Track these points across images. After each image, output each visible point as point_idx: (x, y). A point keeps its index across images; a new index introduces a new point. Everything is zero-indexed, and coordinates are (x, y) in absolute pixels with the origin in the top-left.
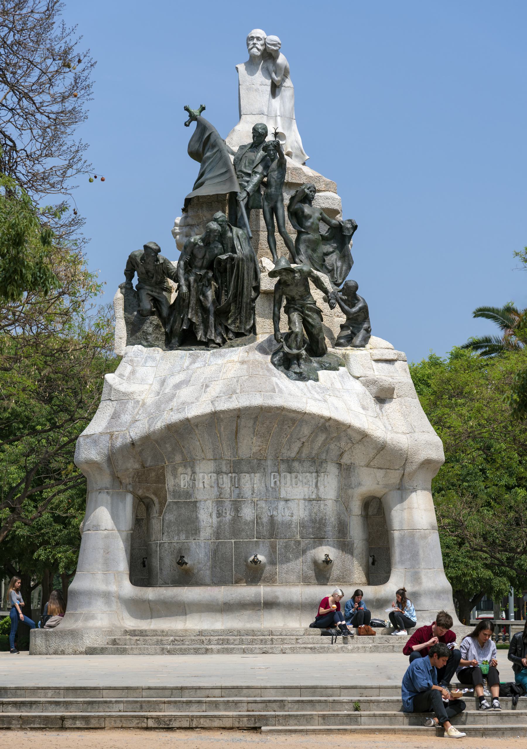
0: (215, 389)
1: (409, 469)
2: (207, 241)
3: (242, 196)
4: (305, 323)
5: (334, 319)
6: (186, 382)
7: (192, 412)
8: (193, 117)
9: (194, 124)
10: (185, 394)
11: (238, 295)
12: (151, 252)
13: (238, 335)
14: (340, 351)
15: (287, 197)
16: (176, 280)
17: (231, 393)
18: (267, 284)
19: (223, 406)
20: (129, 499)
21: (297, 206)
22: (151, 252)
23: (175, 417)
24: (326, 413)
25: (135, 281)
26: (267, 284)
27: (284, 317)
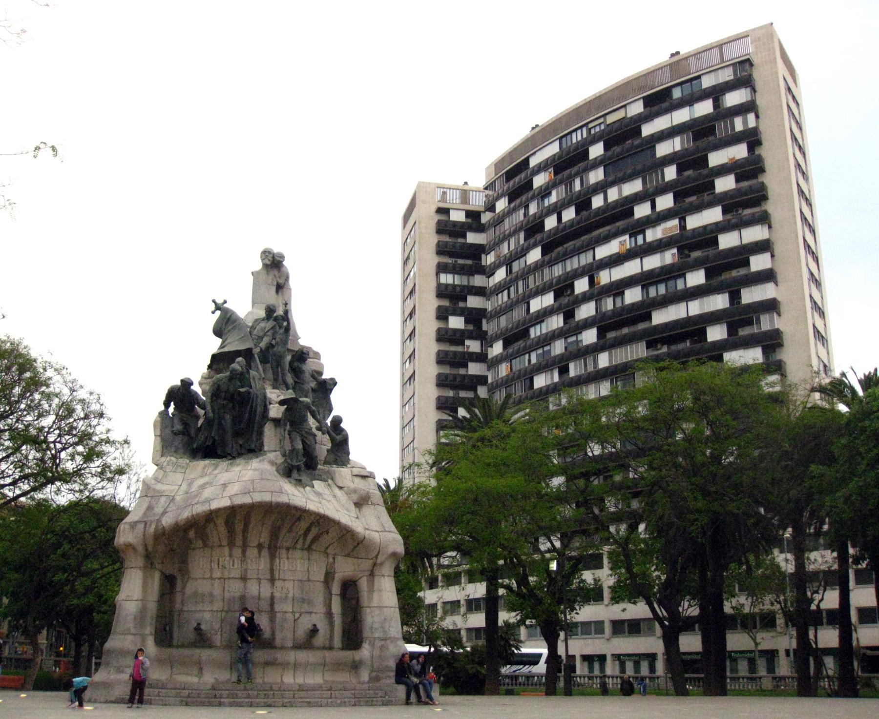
0: (234, 489)
2: (231, 379)
3: (256, 351)
4: (303, 442)
5: (323, 444)
7: (214, 505)
9: (218, 313)
10: (207, 493)
11: (251, 421)
12: (186, 384)
14: (326, 468)
16: (203, 407)
18: (276, 411)
19: (239, 501)
20: (157, 575)
21: (296, 364)
22: (186, 384)
23: (200, 509)
24: (322, 511)
25: (171, 409)
26: (276, 411)
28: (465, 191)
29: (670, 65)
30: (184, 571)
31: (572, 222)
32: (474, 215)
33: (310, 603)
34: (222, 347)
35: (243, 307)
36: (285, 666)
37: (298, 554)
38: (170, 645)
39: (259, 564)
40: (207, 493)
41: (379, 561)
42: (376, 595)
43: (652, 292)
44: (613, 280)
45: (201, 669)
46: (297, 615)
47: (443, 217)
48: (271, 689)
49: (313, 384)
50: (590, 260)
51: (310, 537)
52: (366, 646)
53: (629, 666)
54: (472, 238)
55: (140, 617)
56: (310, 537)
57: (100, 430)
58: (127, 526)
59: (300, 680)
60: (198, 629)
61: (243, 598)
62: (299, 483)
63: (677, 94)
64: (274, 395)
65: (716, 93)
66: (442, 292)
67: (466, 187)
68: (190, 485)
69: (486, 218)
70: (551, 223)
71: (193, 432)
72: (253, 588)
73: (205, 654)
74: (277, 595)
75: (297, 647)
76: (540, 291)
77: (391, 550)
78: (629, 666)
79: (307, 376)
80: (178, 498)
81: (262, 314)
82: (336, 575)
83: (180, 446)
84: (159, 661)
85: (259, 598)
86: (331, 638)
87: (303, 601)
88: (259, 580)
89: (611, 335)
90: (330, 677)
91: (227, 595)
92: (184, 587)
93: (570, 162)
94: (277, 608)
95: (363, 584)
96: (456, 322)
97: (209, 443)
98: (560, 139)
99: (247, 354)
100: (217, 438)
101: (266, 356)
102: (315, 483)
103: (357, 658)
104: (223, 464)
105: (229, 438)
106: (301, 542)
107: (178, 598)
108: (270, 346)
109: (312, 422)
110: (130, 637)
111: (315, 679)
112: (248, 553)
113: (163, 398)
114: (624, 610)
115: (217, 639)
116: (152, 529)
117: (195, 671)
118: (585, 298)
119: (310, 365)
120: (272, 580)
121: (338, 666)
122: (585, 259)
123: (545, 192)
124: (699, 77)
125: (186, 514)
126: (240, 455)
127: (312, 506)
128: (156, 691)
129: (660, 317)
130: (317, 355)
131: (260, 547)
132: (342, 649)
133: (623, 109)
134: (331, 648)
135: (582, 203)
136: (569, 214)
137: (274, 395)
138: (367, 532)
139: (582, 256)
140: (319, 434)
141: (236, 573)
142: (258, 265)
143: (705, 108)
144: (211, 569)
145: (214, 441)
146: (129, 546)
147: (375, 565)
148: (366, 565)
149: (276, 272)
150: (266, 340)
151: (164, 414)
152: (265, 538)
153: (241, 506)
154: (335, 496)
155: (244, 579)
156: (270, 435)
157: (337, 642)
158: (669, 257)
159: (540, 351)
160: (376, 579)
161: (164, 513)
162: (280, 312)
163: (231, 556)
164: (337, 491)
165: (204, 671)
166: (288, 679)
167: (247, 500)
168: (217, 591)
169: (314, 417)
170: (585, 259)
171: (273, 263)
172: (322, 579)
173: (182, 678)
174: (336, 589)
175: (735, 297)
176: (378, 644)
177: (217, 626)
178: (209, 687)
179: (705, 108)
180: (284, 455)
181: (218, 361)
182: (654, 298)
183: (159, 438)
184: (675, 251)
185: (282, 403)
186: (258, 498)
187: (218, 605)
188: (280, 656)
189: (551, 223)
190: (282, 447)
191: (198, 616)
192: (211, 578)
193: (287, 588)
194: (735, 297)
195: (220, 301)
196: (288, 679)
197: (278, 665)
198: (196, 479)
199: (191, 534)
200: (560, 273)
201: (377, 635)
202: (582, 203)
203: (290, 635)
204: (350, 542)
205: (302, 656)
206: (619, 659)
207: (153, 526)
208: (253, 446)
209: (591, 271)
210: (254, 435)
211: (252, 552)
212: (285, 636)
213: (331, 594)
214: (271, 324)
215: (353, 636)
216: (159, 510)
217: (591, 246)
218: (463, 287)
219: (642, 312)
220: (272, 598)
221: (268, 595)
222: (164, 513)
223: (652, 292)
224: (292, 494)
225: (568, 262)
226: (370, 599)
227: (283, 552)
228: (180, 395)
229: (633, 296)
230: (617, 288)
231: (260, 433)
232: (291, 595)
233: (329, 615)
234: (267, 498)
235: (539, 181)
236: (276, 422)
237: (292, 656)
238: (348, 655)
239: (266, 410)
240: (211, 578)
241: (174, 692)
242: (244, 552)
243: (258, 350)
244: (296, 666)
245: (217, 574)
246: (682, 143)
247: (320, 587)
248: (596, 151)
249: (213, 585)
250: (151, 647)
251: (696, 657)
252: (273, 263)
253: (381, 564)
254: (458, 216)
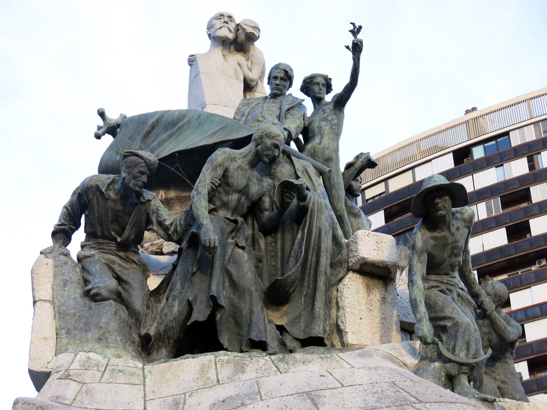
11: (309, 269)
13: (317, 342)
29: (467, 122)
63: (478, 153)
65: (530, 151)
83: (113, 325)
100: (222, 301)
124: (507, 134)
133: (411, 171)
143: (519, 168)
145: (215, 305)
149: (239, 57)
179: (519, 168)
183: (47, 310)
195: (113, 116)
208: (318, 330)
246: (489, 209)
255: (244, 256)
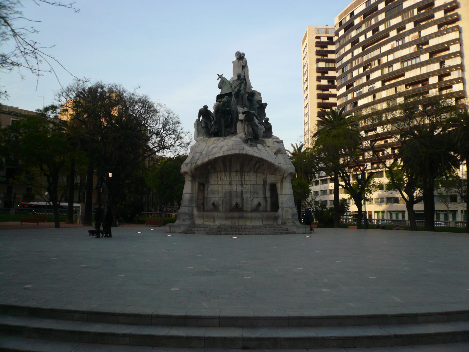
0: (225, 149)
1: (285, 175)
4: (253, 129)
5: (262, 129)
6: (216, 147)
7: (217, 156)
8: (220, 78)
9: (220, 79)
12: (206, 107)
14: (263, 139)
15: (247, 95)
16: (213, 117)
17: (229, 150)
19: (227, 153)
20: (197, 184)
21: (250, 98)
22: (206, 107)
23: (211, 157)
24: (260, 157)
25: (201, 118)
26: (241, 117)
27: (246, 128)
28: (327, 29)
30: (208, 182)
31: (371, 38)
32: (330, 39)
33: (257, 193)
34: (221, 92)
35: (229, 76)
36: (247, 218)
37: (252, 174)
38: (204, 211)
39: (236, 178)
40: (215, 150)
41: (285, 176)
42: (284, 190)
43: (405, 64)
44: (389, 60)
45: (214, 220)
46: (252, 198)
47: (318, 40)
48: (241, 228)
49: (258, 106)
50: (379, 53)
51: (256, 168)
52: (280, 210)
53: (394, 215)
54: (330, 48)
55: (191, 200)
56: (256, 168)
57: (179, 129)
58: (185, 165)
59: (253, 224)
60: (213, 204)
61: (230, 192)
62: (251, 145)
64: (240, 110)
66: (319, 70)
67: (327, 27)
68: (209, 147)
69: (335, 39)
70: (362, 39)
71: (209, 126)
72: (234, 188)
73: (216, 214)
74: (244, 190)
75: (253, 211)
76: (357, 67)
77: (290, 171)
78: (394, 215)
79: (255, 102)
80: (203, 153)
81: (236, 78)
82: (268, 182)
84: (199, 217)
85: (237, 192)
86: (266, 207)
87: (254, 192)
88: (236, 185)
89: (387, 84)
90: (265, 223)
91: (224, 191)
92: (207, 188)
93: (371, 11)
94: (244, 195)
95: (279, 185)
96: (324, 82)
97: (216, 130)
98: (366, 2)
99: (229, 95)
101: (238, 95)
102: (258, 145)
103: (276, 215)
104: (221, 139)
105: (223, 128)
106: (253, 169)
107: (206, 192)
108: (239, 91)
109: (256, 121)
110: (187, 208)
111: (258, 223)
112: (232, 175)
113: (198, 114)
114: (391, 193)
115: (221, 208)
116: (193, 166)
117: (212, 221)
118: (376, 69)
119: (256, 97)
120: (242, 185)
121: (268, 218)
122: (377, 52)
123: (359, 26)
125: (206, 160)
126: (228, 135)
127: (256, 155)
128: (197, 229)
129: (409, 75)
130: (259, 94)
131: (237, 172)
132: (271, 211)
134: (266, 211)
135: (375, 29)
136: (370, 34)
137: (240, 110)
138: (279, 165)
139: (375, 51)
140: (259, 125)
141: (227, 182)
142: (235, 59)
144: (218, 181)
146: (186, 173)
147: (283, 178)
148: (279, 177)
150: (237, 88)
151: (198, 120)
152: (238, 168)
153: (228, 156)
154: (266, 150)
155: (231, 184)
156: (240, 126)
157: (269, 209)
158: (412, 49)
159: (358, 92)
160: (284, 183)
161: (198, 159)
162: (242, 77)
163: (225, 176)
164: (267, 148)
165: (216, 221)
166: (249, 223)
167: (229, 153)
168: (220, 189)
169: (257, 118)
170: (377, 52)
171: (240, 57)
172: (262, 184)
173: (207, 223)
174: (268, 187)
175: (442, 63)
176: (285, 209)
177: (221, 203)
178: (217, 227)
180: (245, 134)
181: (219, 97)
182: (406, 67)
184: (415, 46)
185: (243, 113)
186: (234, 152)
187: (221, 195)
188: (245, 215)
189: (362, 39)
190: (245, 131)
191: (213, 199)
192: (218, 184)
193: (248, 187)
194: (442, 63)
196: (249, 223)
197: (244, 218)
198: (210, 145)
199: (209, 167)
200: (366, 59)
201: (284, 206)
202: (375, 29)
203: (250, 206)
204: (272, 169)
205: (254, 215)
206: (390, 213)
207: (194, 164)
208: (233, 131)
209: (378, 58)
210: (233, 128)
211: (233, 174)
212: (247, 207)
213: (266, 190)
214: (239, 82)
215: (275, 206)
216: (196, 158)
217: (379, 46)
218: (326, 68)
219: (401, 73)
220: (242, 191)
221: (241, 190)
222: (198, 159)
223: (405, 64)
224: (249, 150)
225: (369, 54)
226: (281, 191)
227: (246, 174)
228: (204, 112)
229: (397, 66)
230: (390, 64)
231: (236, 126)
232: (249, 190)
233: (265, 198)
234: (237, 152)
235: (357, 21)
236: (242, 121)
237: (249, 215)
238: (273, 214)
239: (238, 116)
240: (218, 184)
241: (204, 229)
242: (230, 174)
243: (234, 92)
244: (251, 218)
245: (220, 183)
247: (262, 187)
248: (382, 6)
249: (218, 187)
250: (196, 212)
251: (422, 212)
252: (240, 57)
253: (286, 177)
254: (324, 39)
255: (223, 120)
